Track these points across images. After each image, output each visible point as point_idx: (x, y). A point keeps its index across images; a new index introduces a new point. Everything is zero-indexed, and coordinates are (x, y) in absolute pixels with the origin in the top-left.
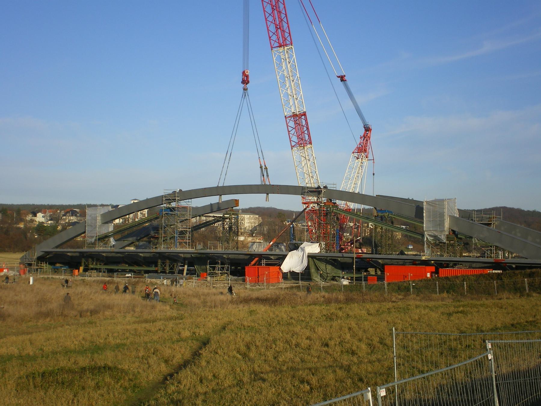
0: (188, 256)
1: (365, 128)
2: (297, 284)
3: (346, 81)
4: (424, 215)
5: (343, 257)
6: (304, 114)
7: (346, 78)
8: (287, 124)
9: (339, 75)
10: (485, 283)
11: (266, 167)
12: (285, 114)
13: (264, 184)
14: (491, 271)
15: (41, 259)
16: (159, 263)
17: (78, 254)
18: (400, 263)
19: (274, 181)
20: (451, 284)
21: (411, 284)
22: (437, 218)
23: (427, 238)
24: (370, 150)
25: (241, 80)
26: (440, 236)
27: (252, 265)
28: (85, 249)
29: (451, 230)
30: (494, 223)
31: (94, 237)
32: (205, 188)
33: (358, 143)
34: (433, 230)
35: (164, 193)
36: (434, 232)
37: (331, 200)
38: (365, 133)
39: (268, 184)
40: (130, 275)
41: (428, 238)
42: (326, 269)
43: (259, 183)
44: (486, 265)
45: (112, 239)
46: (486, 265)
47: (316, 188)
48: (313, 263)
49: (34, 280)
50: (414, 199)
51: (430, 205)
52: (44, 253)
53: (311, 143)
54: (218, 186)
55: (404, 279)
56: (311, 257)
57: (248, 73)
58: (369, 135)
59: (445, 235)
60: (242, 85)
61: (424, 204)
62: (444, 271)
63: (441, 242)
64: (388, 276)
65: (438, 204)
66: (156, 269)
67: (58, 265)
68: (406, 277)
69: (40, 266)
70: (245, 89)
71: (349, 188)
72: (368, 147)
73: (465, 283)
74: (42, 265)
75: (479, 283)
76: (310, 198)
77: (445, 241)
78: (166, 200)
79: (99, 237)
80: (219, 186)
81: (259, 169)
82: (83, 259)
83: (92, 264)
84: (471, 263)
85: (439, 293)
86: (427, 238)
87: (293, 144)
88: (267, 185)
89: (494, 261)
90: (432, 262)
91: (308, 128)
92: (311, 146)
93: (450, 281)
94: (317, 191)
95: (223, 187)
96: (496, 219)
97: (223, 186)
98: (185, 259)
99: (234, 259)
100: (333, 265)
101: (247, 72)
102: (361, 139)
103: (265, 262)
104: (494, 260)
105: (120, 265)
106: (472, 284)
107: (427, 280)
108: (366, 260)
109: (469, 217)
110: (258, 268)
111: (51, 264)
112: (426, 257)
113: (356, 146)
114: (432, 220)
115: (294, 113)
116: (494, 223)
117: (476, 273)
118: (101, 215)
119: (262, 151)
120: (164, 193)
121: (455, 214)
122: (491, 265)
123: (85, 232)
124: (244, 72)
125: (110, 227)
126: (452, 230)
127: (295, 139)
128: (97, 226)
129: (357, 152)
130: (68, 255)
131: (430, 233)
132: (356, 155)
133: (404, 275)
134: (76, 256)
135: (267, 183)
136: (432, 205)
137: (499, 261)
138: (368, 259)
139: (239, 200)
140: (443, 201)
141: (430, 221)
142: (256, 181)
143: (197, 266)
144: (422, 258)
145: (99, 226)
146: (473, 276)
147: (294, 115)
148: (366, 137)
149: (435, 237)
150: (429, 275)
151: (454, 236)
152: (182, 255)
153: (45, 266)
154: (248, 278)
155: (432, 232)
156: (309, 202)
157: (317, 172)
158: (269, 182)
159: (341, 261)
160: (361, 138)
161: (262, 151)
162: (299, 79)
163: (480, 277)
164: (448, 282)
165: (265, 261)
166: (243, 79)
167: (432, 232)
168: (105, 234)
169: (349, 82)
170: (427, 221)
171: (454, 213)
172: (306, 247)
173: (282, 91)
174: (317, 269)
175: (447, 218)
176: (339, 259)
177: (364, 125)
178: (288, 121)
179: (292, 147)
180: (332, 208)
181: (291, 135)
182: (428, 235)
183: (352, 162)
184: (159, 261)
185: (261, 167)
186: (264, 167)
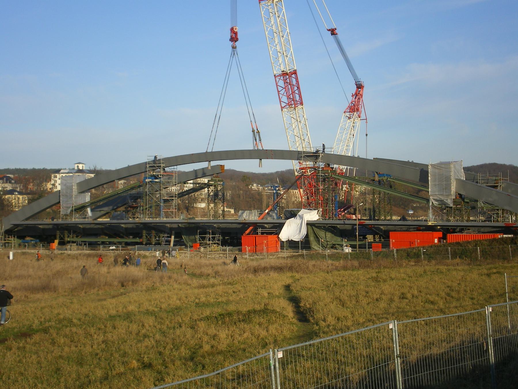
0: (175, 226)
1: (356, 85)
2: (297, 252)
3: (337, 34)
4: (429, 179)
5: (345, 224)
6: (295, 72)
7: (336, 31)
8: (277, 84)
9: (330, 28)
10: (498, 248)
11: (258, 131)
12: (275, 73)
13: (256, 149)
14: (501, 236)
15: (9, 232)
16: (144, 235)
17: (51, 227)
18: (404, 229)
19: (267, 145)
20: (463, 249)
21: (422, 250)
22: (443, 182)
23: (432, 202)
24: (363, 109)
25: (230, 38)
26: (446, 200)
27: (247, 235)
28: (60, 221)
29: (457, 194)
30: (500, 186)
31: (70, 207)
32: (192, 154)
33: (350, 102)
34: (439, 195)
35: (148, 159)
36: (440, 197)
37: (329, 165)
38: (356, 91)
39: (261, 149)
40: (114, 248)
41: (434, 202)
42: (326, 236)
43: (251, 147)
44: (495, 229)
45: (89, 210)
46: (495, 229)
47: (314, 153)
48: (312, 231)
49: (14, 255)
50: (414, 162)
51: (436, 168)
52: (13, 225)
53: (302, 104)
54: (207, 152)
55: (410, 246)
56: (310, 225)
57: (237, 29)
58: (361, 93)
59: (451, 199)
60: (231, 43)
61: (429, 167)
62: (453, 237)
63: (448, 207)
64: (393, 243)
65: (443, 167)
66: (141, 240)
67: (28, 239)
68: (412, 243)
69: (8, 240)
70: (234, 48)
71: (342, 151)
72: (360, 106)
73: (479, 248)
74: (10, 239)
75: (492, 248)
76: (308, 163)
77: (451, 205)
78: (150, 167)
79: (76, 207)
80: (208, 151)
81: (252, 133)
82: (58, 231)
83: (68, 237)
84: (479, 228)
85: (452, 259)
86: (432, 202)
87: (283, 105)
88: (260, 150)
89: (504, 225)
90: (438, 227)
91: (298, 88)
92: (302, 107)
93: (461, 246)
94: (314, 156)
95: (212, 153)
96: (503, 181)
97: (212, 152)
98: (171, 229)
99: (226, 228)
100: (332, 232)
101: (236, 29)
102: (353, 98)
103: (261, 230)
104: (505, 224)
105: (98, 238)
106: (485, 249)
107: (436, 246)
108: (368, 227)
109: (474, 179)
110: (255, 237)
111: (19, 237)
112: (433, 222)
113: (347, 105)
114: (438, 184)
115: (283, 71)
116: (500, 186)
117: (488, 238)
118: (77, 183)
119: (253, 114)
120: (148, 159)
121: (461, 177)
122: (500, 229)
123: (59, 202)
124: (232, 29)
125: (87, 196)
126: (458, 194)
127: (285, 99)
128: (74, 196)
129: (349, 111)
130: (40, 228)
131: (435, 198)
132: (348, 114)
133: (410, 242)
134: (49, 229)
135: (260, 148)
136: (438, 168)
137: (510, 225)
138: (370, 226)
139: (224, 165)
140: (449, 163)
141: (435, 185)
142: (250, 146)
143: (185, 236)
144: (428, 223)
145: (75, 196)
146: (486, 241)
147: (284, 74)
148: (358, 95)
149: (441, 202)
150: (436, 241)
151: (460, 200)
152: (168, 225)
153: (14, 241)
154: (247, 247)
155: (437, 197)
156: (306, 167)
157: (309, 135)
158: (262, 147)
159: (341, 228)
160: (353, 96)
161: (253, 114)
162: (289, 34)
163: (493, 241)
164: (460, 248)
165: (261, 229)
166: (231, 36)
167: (437, 197)
168: (81, 204)
169: (340, 36)
170: (432, 185)
171: (460, 175)
172: (304, 215)
173: (271, 48)
174: (317, 238)
175: (454, 182)
176: (338, 226)
178: (277, 80)
179: (282, 108)
180: (330, 174)
181: (281, 96)
182: (434, 199)
183: (345, 123)
184: (144, 232)
185: (253, 131)
186: (256, 131)
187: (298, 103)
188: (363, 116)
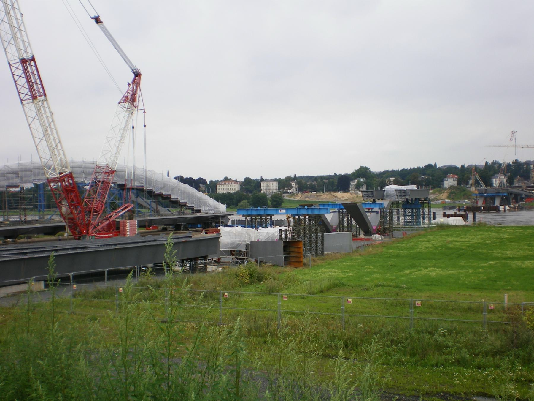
1: (134, 73)
6: (33, 59)
72: (137, 95)
91: (40, 78)
102: (129, 87)
160: (129, 84)
177: (133, 70)
187: (42, 94)
188: (141, 106)
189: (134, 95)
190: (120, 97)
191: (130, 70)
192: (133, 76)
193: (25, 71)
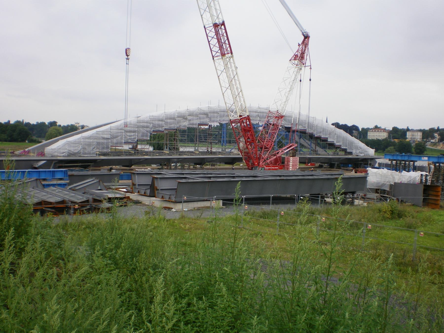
1: (304, 35)
6: (223, 24)
72: (306, 54)
91: (228, 39)
160: (299, 45)
177: (303, 33)
187: (229, 52)
188: (308, 64)
189: (303, 53)
190: (291, 55)
191: (301, 33)
192: (303, 38)
193: (217, 33)
